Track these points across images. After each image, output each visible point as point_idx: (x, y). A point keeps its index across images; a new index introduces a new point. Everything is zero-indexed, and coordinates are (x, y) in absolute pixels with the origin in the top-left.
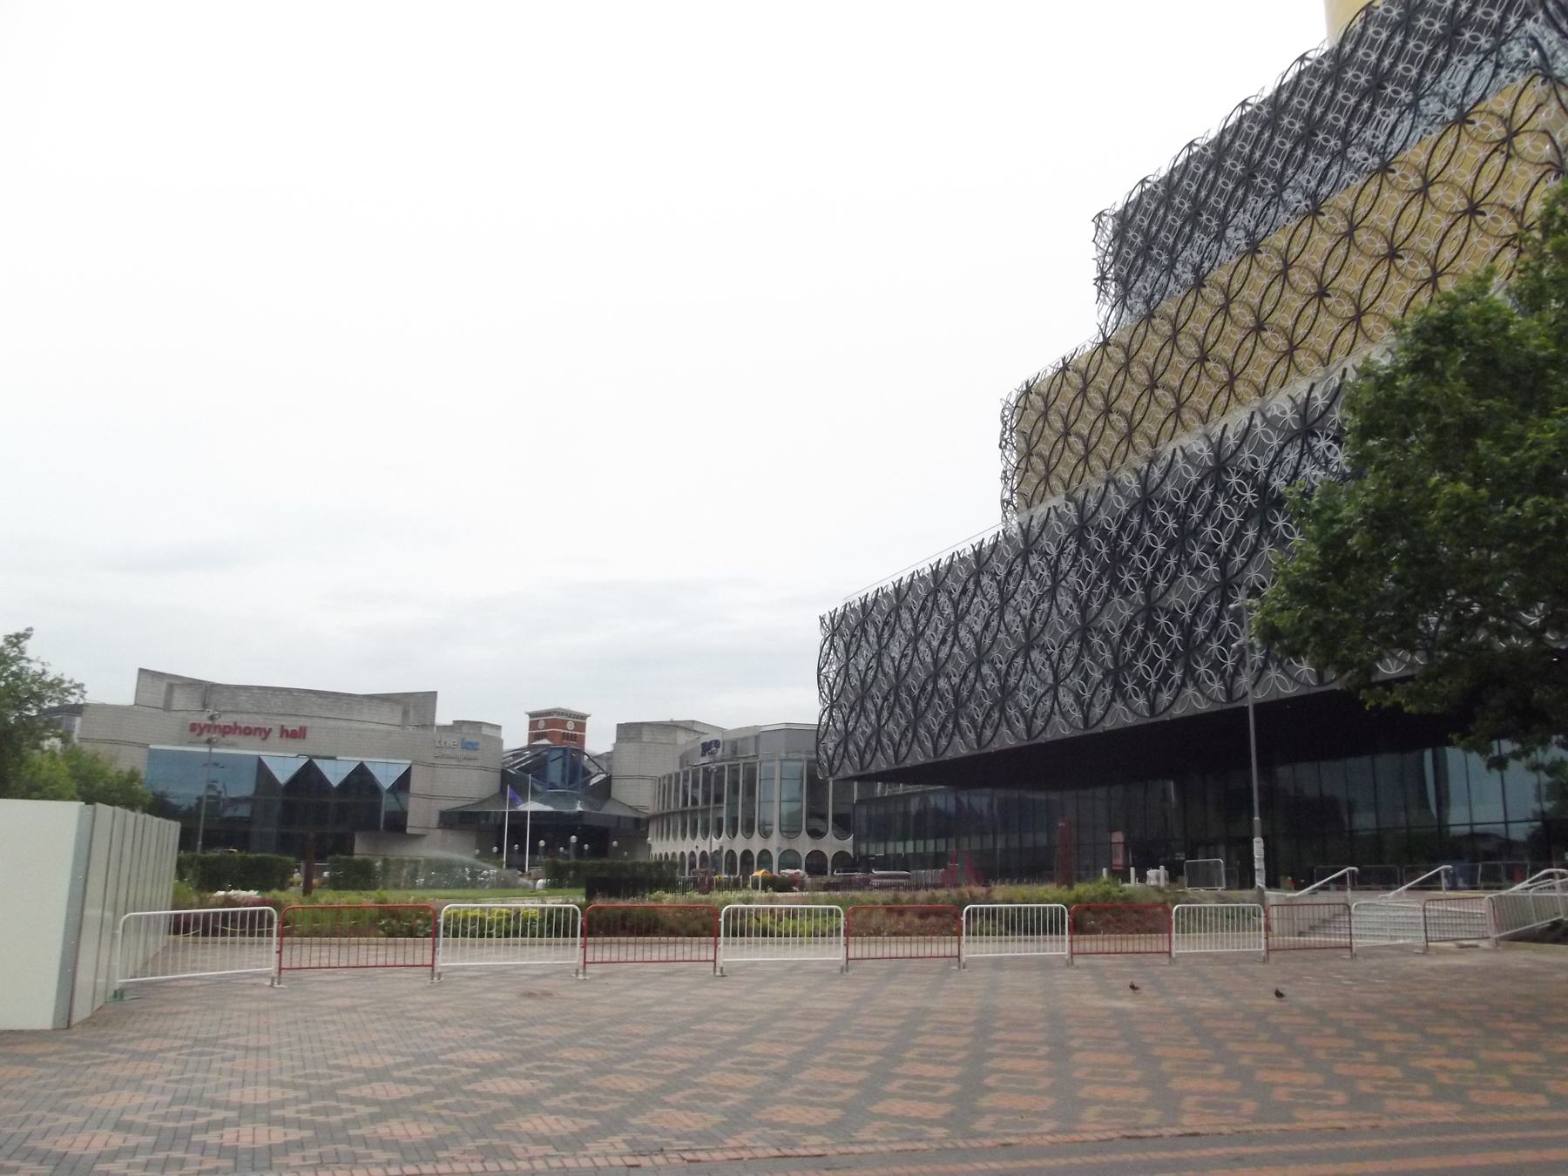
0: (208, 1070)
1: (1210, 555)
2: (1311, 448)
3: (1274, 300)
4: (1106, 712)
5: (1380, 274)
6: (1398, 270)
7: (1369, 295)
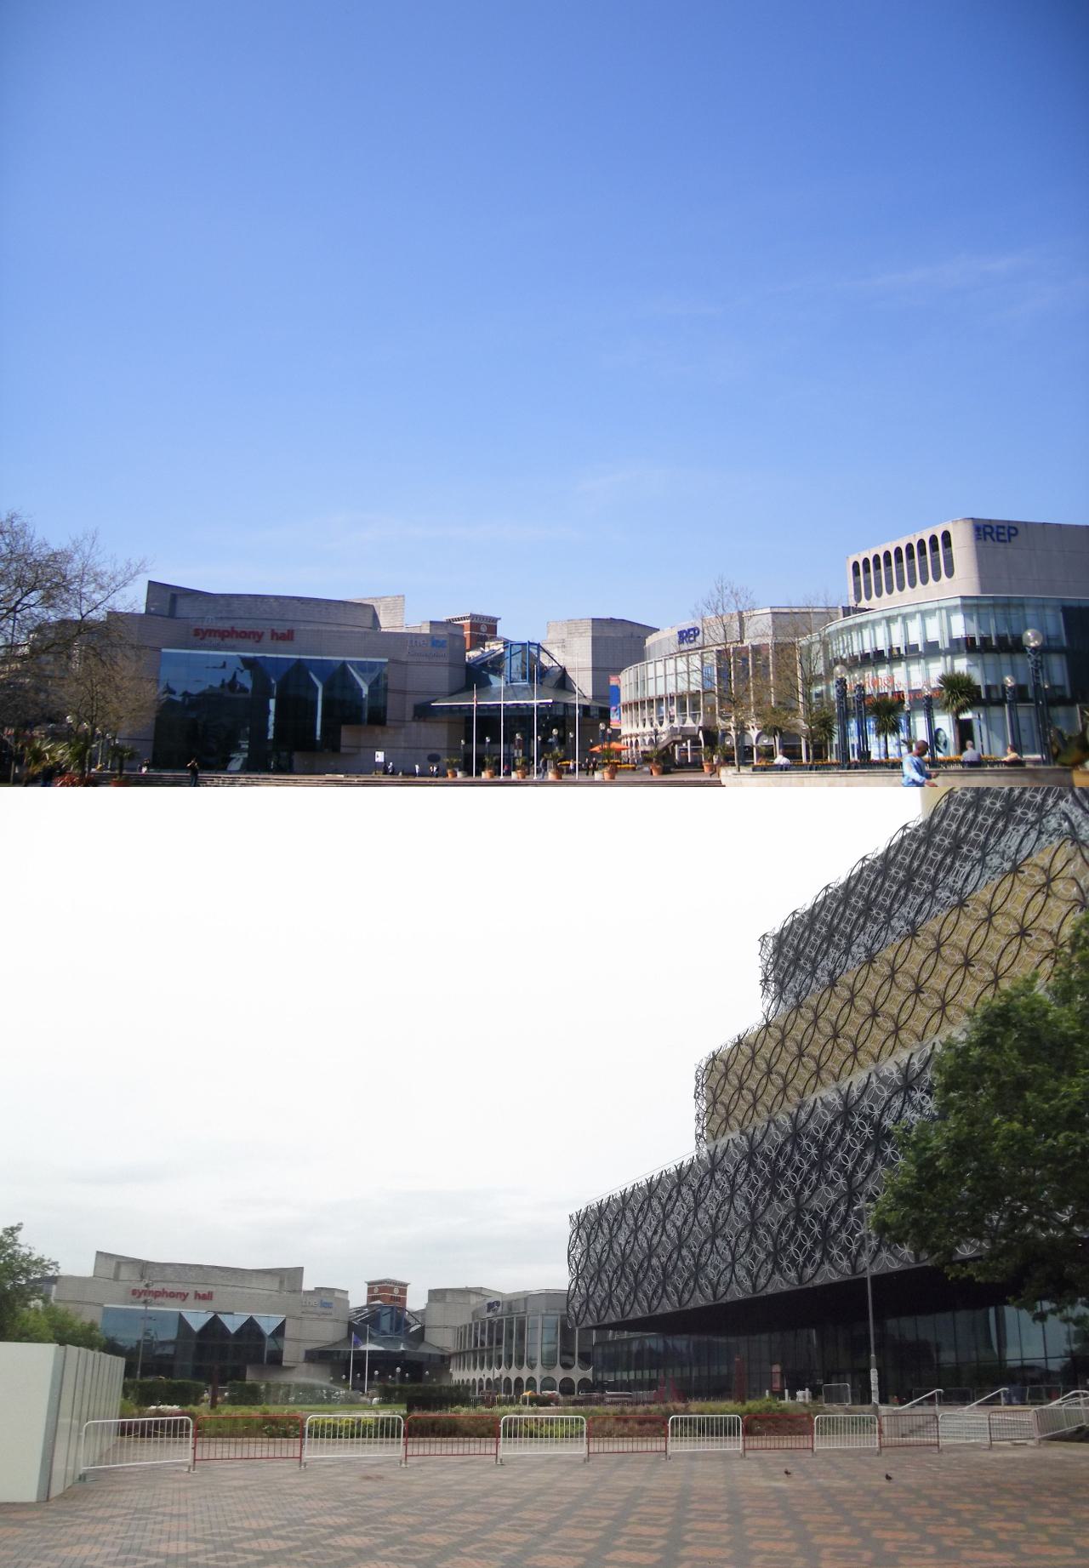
0: (145, 1530)
1: (841, 1172)
2: (910, 1098)
3: (885, 995)
4: (768, 1282)
5: (958, 977)
6: (971, 974)
7: (951, 992)
